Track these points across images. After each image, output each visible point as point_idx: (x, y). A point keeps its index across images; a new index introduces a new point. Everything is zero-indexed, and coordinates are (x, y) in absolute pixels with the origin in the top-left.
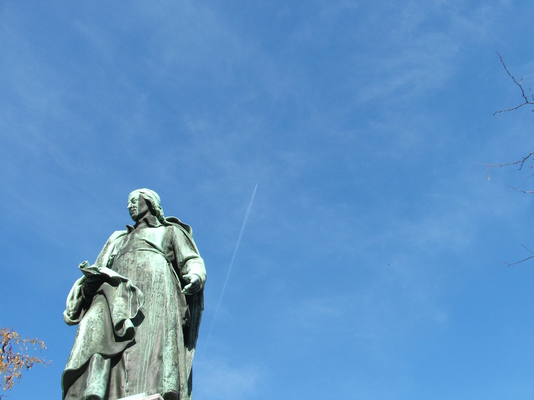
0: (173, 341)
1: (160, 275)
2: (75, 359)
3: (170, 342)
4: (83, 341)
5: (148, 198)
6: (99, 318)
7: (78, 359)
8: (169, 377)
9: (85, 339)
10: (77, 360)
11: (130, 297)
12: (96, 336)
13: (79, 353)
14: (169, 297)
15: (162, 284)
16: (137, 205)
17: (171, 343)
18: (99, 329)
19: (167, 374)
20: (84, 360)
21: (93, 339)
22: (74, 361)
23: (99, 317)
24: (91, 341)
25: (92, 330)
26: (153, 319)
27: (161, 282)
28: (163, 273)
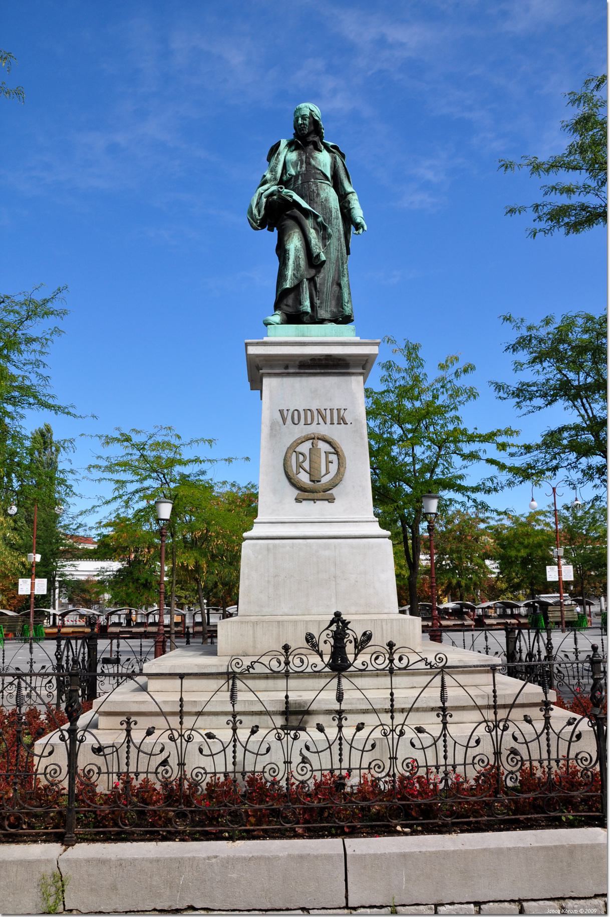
5: (317, 118)
8: (347, 303)
9: (294, 264)
12: (303, 263)
16: (307, 122)
19: (346, 301)
20: (296, 282)
21: (302, 266)
24: (300, 267)
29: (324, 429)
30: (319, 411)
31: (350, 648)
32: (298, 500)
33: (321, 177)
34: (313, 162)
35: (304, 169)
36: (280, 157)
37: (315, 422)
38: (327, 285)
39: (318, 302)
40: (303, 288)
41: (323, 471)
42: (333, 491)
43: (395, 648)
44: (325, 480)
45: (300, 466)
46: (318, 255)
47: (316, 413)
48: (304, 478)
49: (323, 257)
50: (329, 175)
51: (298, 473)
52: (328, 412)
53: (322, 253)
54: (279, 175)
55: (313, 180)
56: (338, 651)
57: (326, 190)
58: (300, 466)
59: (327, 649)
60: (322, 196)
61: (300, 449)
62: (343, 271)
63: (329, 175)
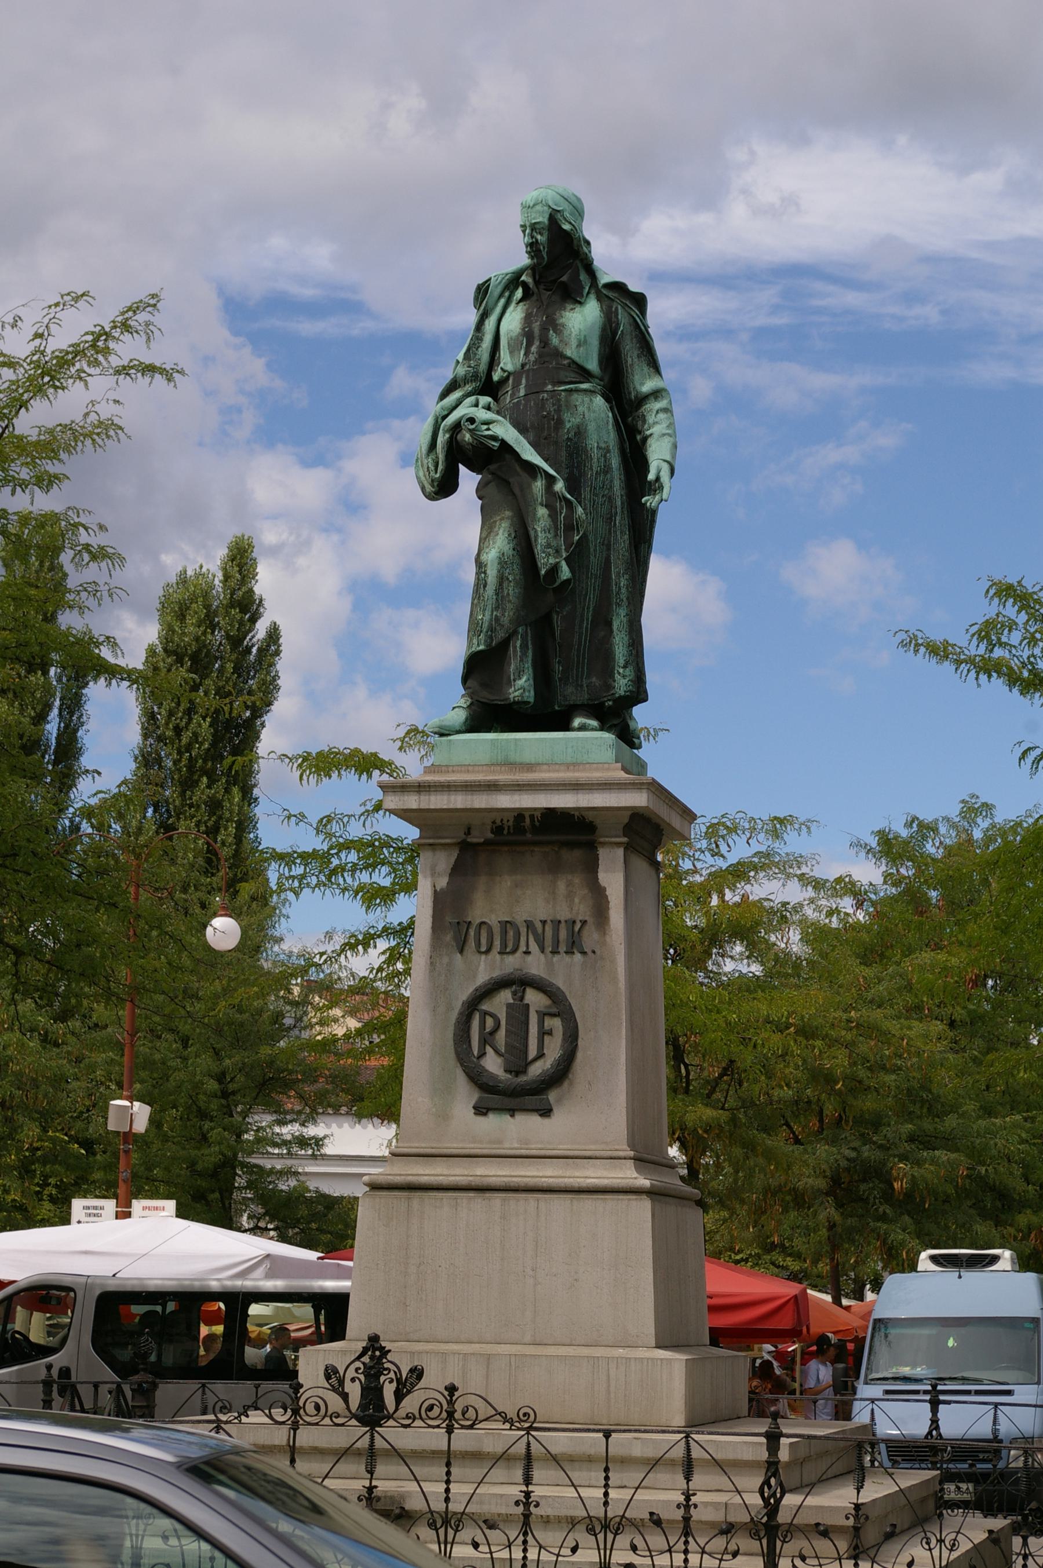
0: (628, 599)
1: (605, 456)
2: (487, 632)
3: (625, 599)
4: (494, 597)
6: (515, 553)
7: (491, 631)
9: (497, 594)
10: (489, 633)
11: (561, 513)
13: (491, 620)
14: (619, 503)
15: (609, 476)
17: (625, 602)
18: (518, 577)
19: (622, 662)
22: (486, 636)
23: (514, 549)
25: (508, 579)
26: (595, 550)
27: (607, 472)
28: (608, 451)
29: (536, 964)
30: (529, 925)
31: (389, 1391)
32: (481, 1110)
33: (572, 376)
34: (555, 340)
35: (532, 358)
36: (487, 322)
37: (523, 948)
38: (581, 627)
39: (558, 668)
40: (515, 647)
41: (532, 1052)
42: (552, 1096)
43: (457, 1394)
44: (536, 1070)
45: (487, 1039)
46: (554, 570)
47: (523, 930)
48: (493, 1064)
49: (565, 573)
50: (593, 365)
51: (482, 1054)
52: (549, 929)
53: (564, 564)
54: (483, 367)
55: (549, 387)
56: (372, 1393)
57: (580, 409)
58: (487, 1039)
59: (354, 1391)
60: (568, 425)
61: (485, 1007)
62: (618, 593)
63: (593, 365)
